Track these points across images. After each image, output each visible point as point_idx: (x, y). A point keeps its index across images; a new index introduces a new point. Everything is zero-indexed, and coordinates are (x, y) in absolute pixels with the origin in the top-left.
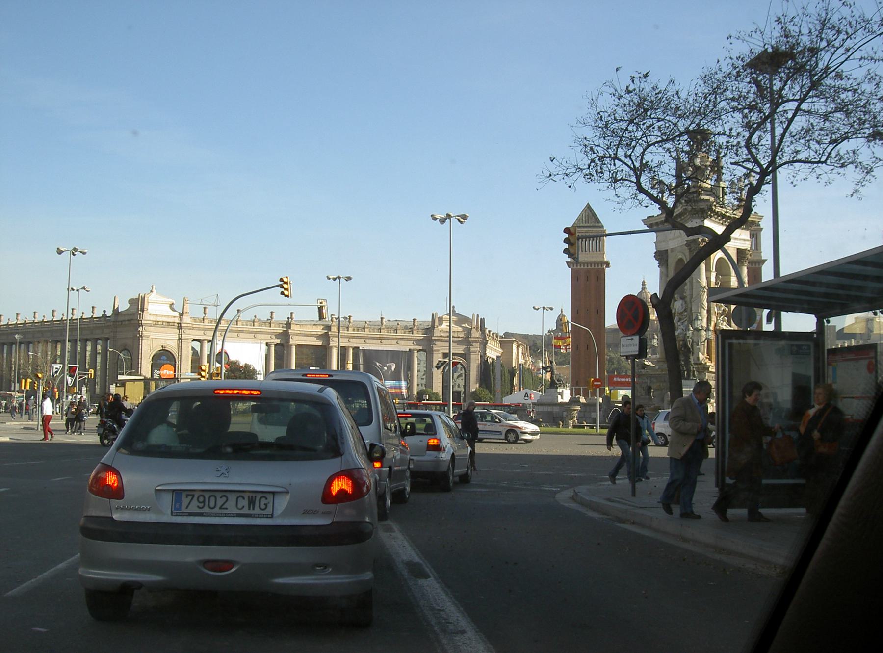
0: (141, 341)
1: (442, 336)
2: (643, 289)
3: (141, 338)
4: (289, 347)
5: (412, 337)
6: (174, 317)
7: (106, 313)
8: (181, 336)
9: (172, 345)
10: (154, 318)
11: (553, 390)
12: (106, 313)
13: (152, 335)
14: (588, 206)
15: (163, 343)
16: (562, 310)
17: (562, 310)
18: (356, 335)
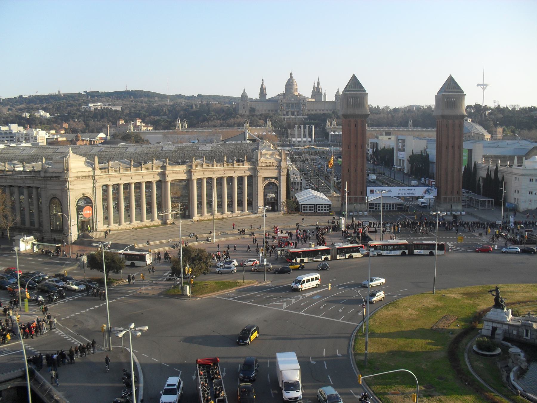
0: (68, 193)
1: (263, 166)
2: (291, 77)
3: (68, 191)
4: (166, 182)
5: (244, 168)
6: (89, 171)
7: (35, 169)
8: (95, 185)
9: (89, 193)
10: (75, 175)
11: (500, 310)
12: (35, 169)
13: (76, 187)
14: (354, 78)
15: (83, 192)
16: (244, 89)
17: (244, 89)
18: (208, 169)
